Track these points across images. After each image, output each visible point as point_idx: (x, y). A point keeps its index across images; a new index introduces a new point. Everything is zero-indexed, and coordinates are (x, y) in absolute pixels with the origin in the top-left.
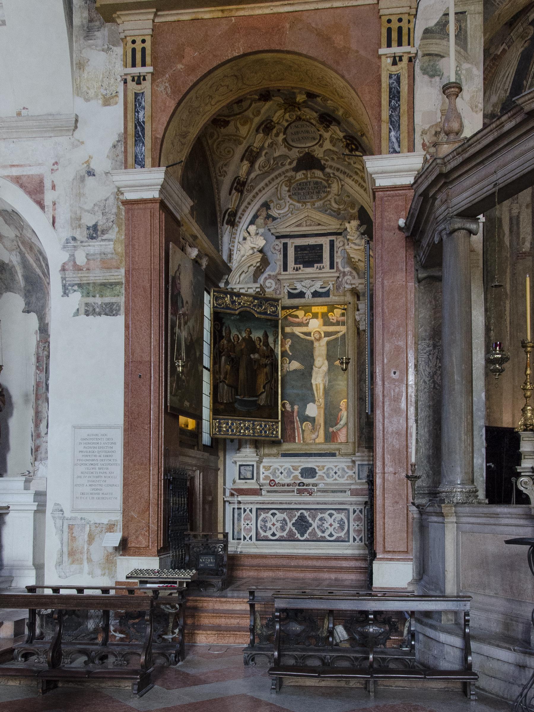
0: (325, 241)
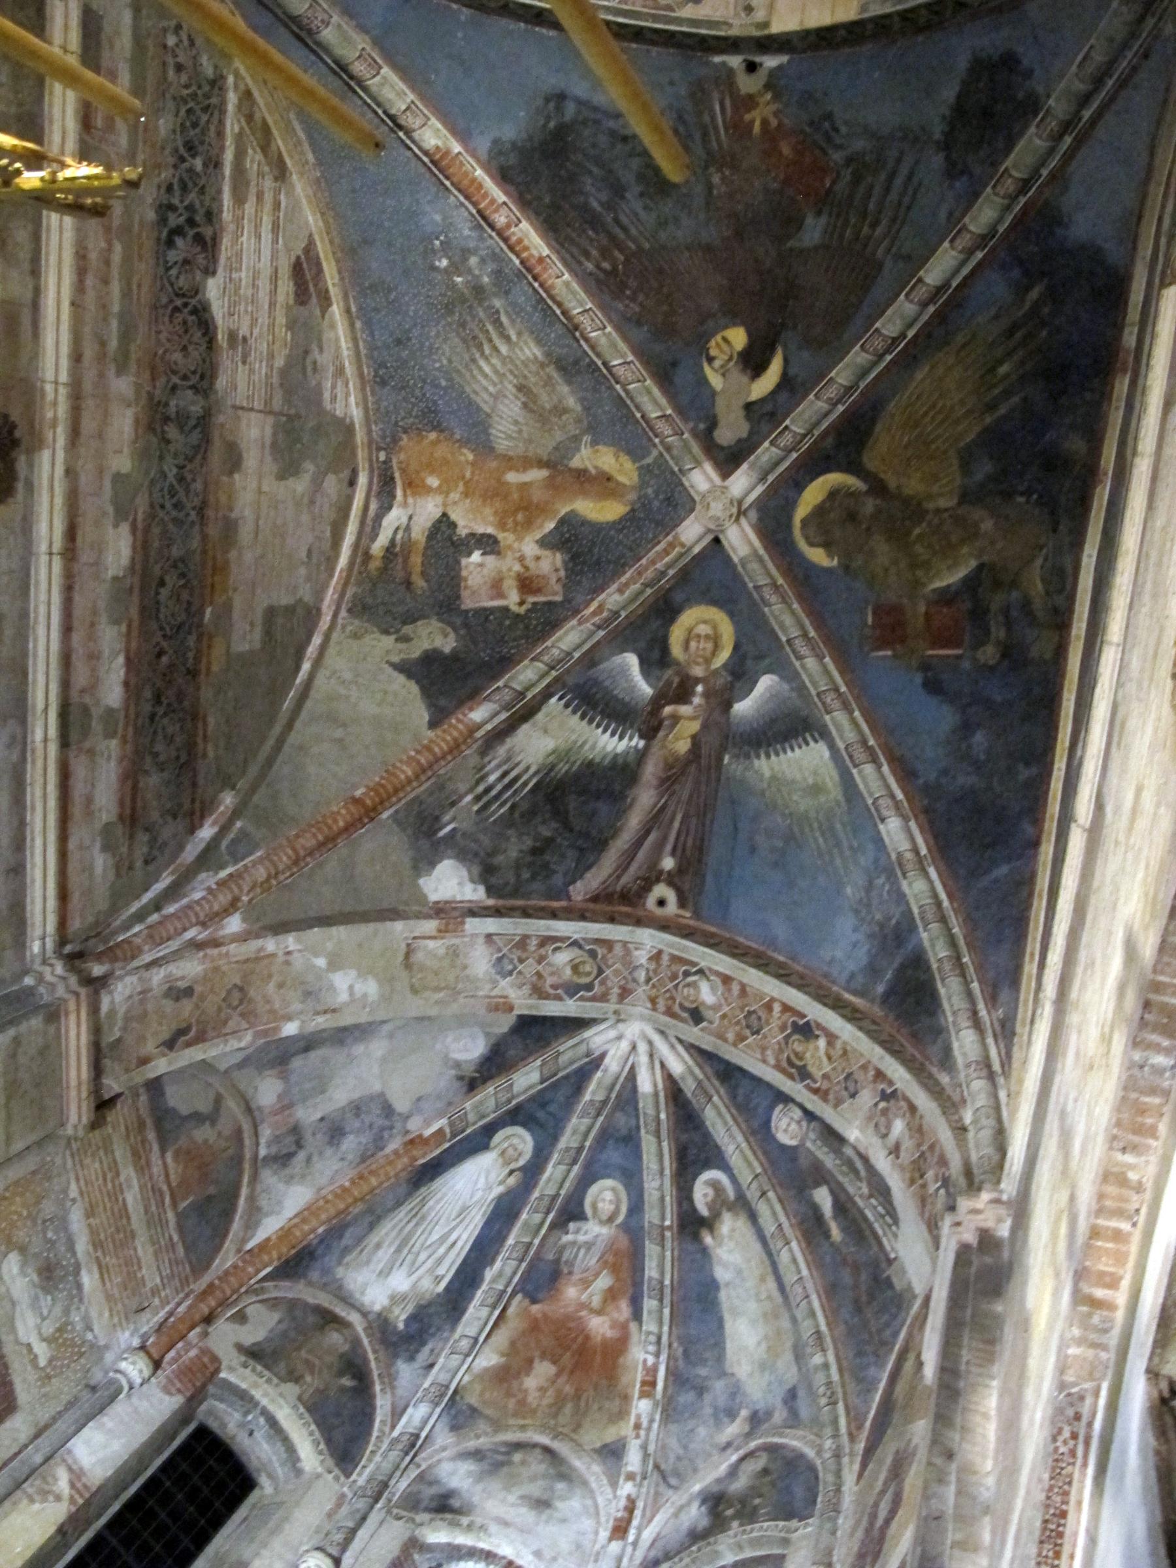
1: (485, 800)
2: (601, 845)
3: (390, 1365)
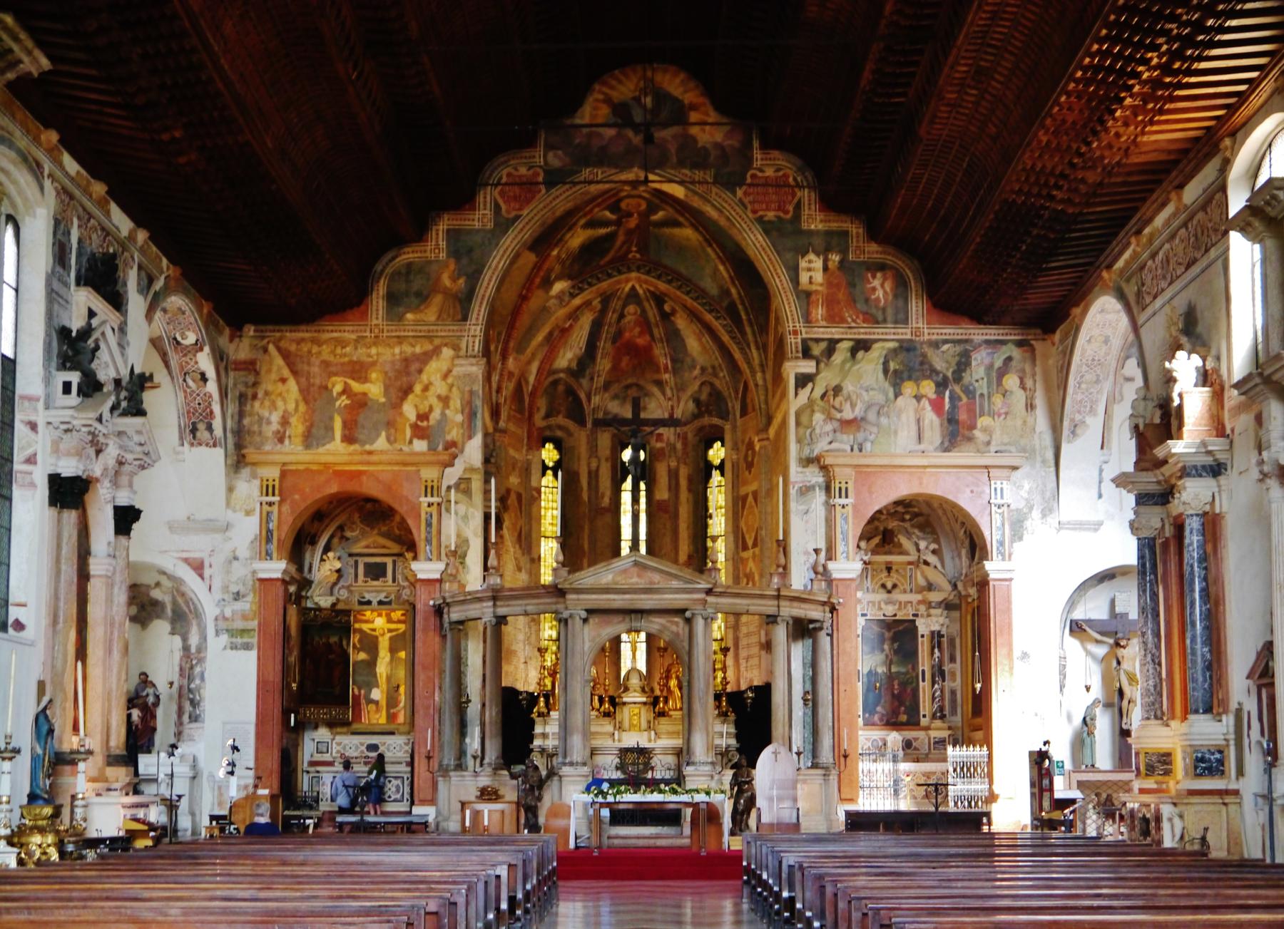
0: (389, 561)
1: (563, 263)
2: (608, 251)
3: (578, 381)
